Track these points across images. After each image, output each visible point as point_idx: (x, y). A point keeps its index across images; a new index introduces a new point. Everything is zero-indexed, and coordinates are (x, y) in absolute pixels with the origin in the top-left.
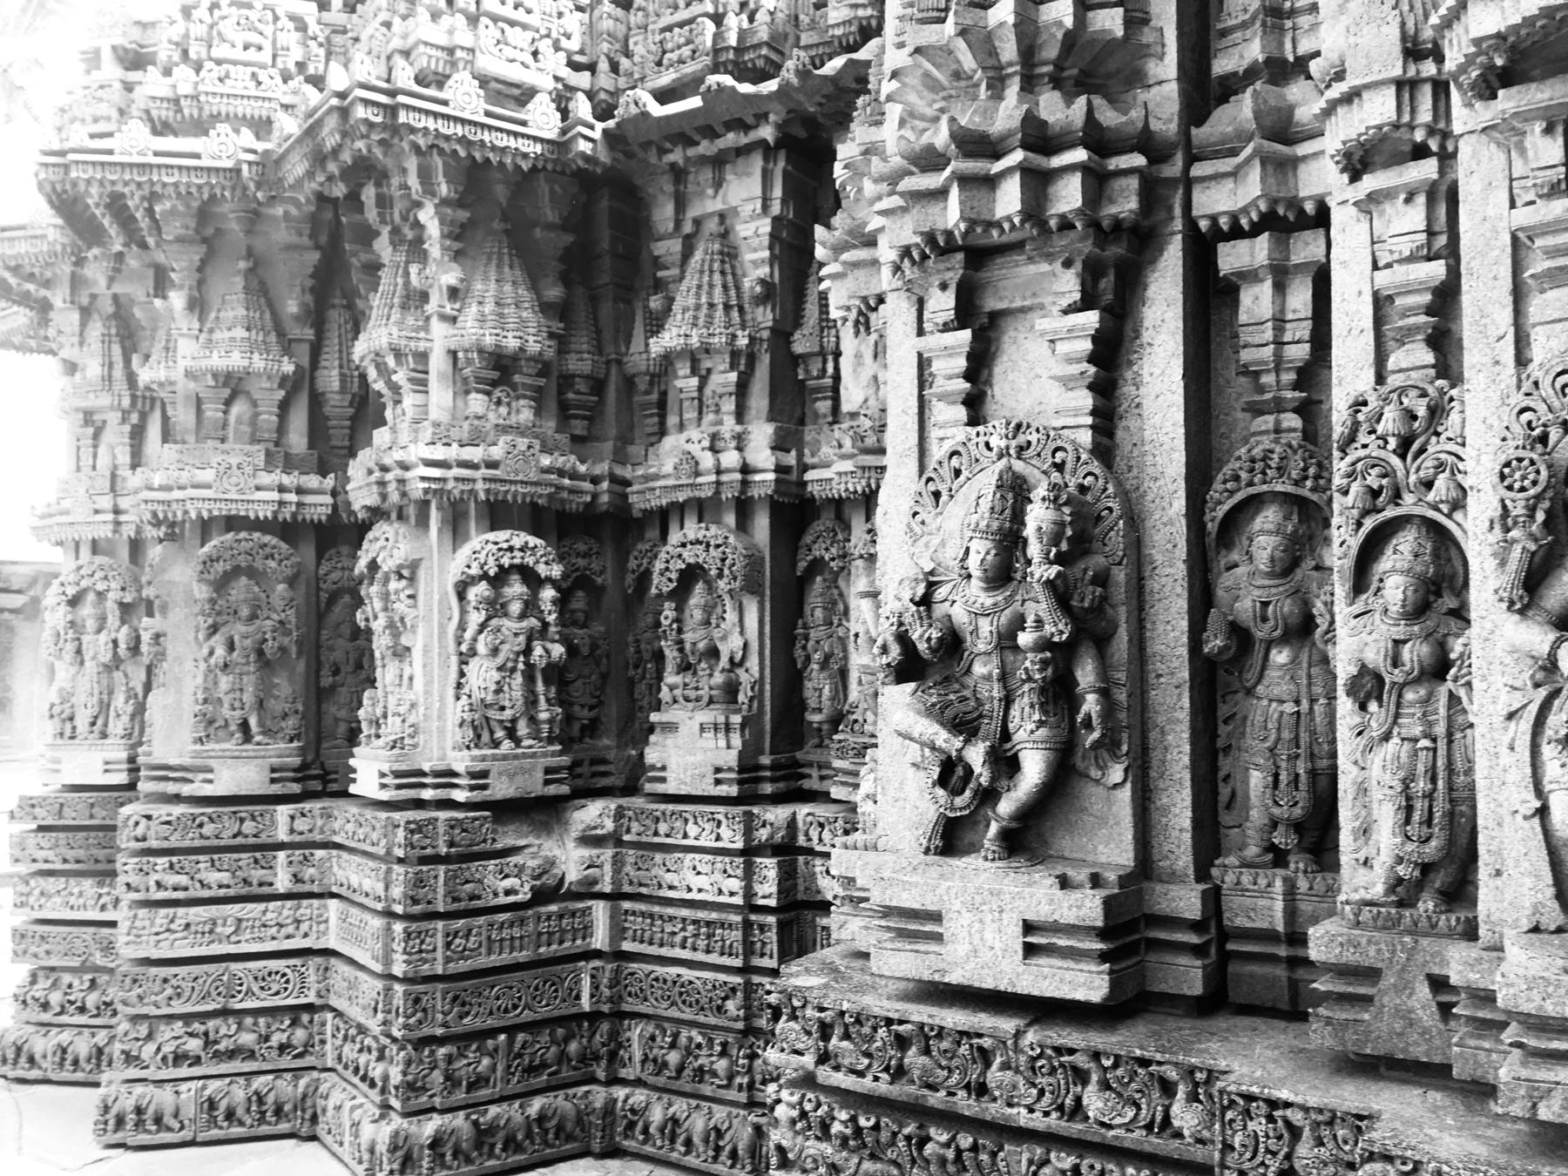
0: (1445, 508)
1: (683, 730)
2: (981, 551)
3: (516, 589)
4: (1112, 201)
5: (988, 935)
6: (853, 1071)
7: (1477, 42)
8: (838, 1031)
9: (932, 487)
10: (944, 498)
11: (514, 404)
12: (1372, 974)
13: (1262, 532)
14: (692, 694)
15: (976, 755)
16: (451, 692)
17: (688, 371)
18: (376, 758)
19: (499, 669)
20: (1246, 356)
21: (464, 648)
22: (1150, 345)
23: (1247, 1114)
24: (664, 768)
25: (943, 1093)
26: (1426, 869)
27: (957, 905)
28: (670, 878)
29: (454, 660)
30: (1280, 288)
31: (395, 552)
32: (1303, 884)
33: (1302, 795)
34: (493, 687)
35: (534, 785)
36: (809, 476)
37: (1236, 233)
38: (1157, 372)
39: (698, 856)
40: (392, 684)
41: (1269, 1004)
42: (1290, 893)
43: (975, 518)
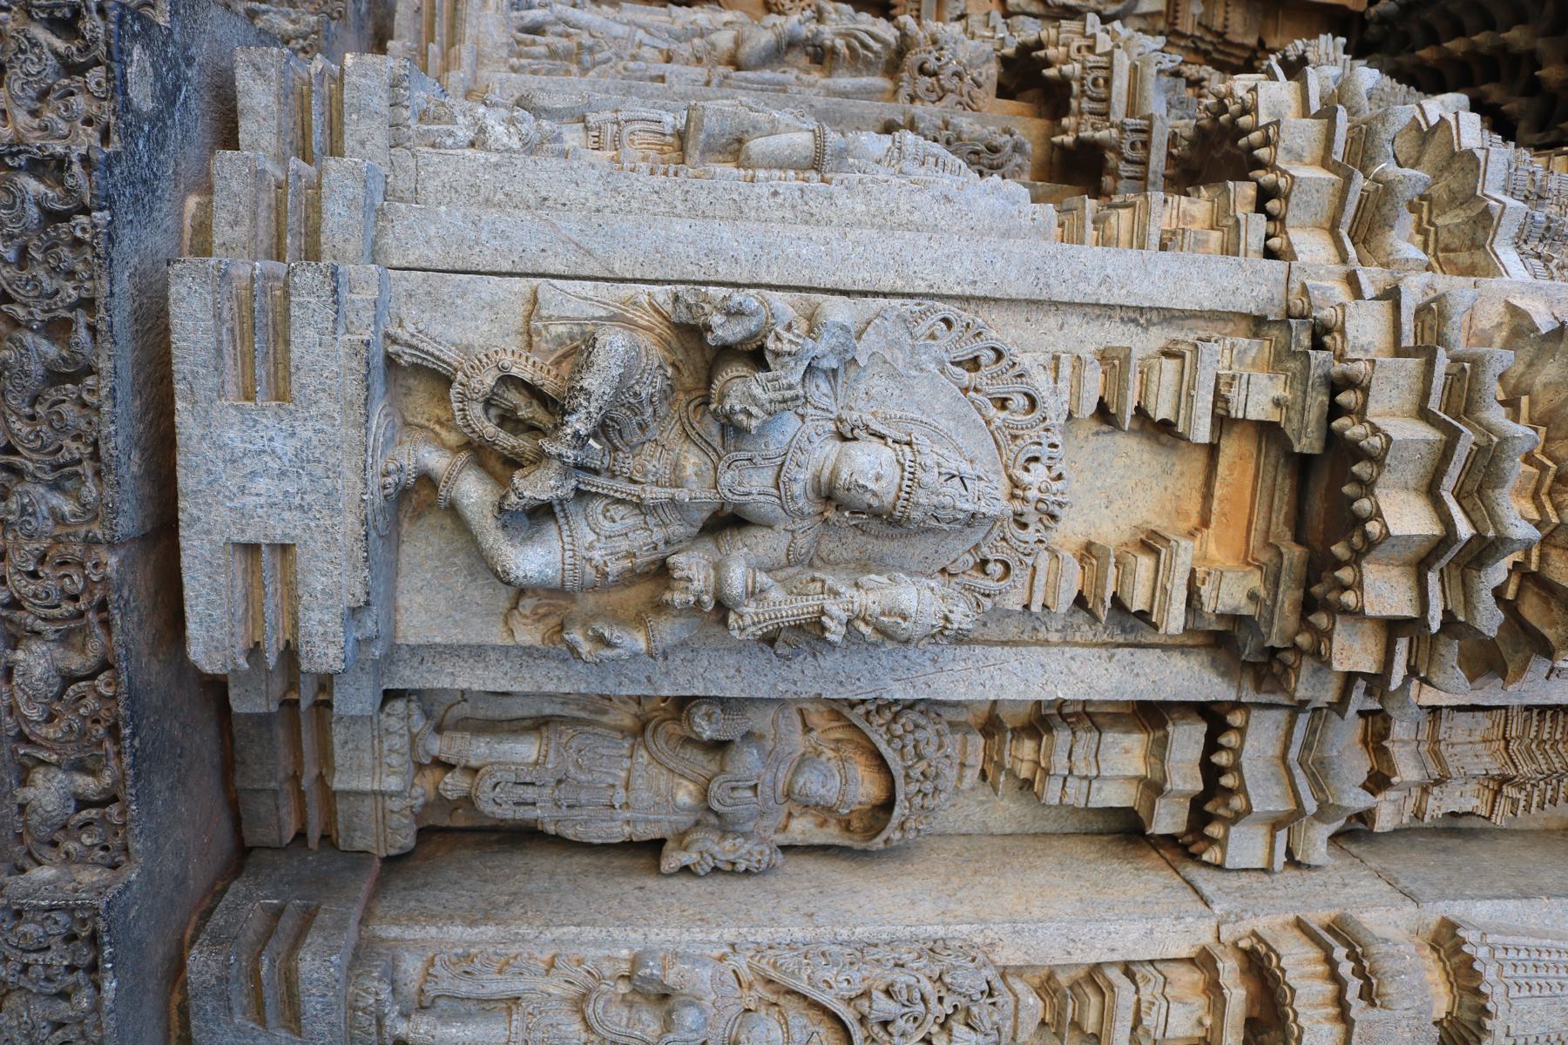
5: (262, 484)
9: (987, 357)
10: (967, 377)
22: (1111, 657)
32: (395, 804)
37: (1211, 746)
38: (1074, 666)
41: (238, 758)
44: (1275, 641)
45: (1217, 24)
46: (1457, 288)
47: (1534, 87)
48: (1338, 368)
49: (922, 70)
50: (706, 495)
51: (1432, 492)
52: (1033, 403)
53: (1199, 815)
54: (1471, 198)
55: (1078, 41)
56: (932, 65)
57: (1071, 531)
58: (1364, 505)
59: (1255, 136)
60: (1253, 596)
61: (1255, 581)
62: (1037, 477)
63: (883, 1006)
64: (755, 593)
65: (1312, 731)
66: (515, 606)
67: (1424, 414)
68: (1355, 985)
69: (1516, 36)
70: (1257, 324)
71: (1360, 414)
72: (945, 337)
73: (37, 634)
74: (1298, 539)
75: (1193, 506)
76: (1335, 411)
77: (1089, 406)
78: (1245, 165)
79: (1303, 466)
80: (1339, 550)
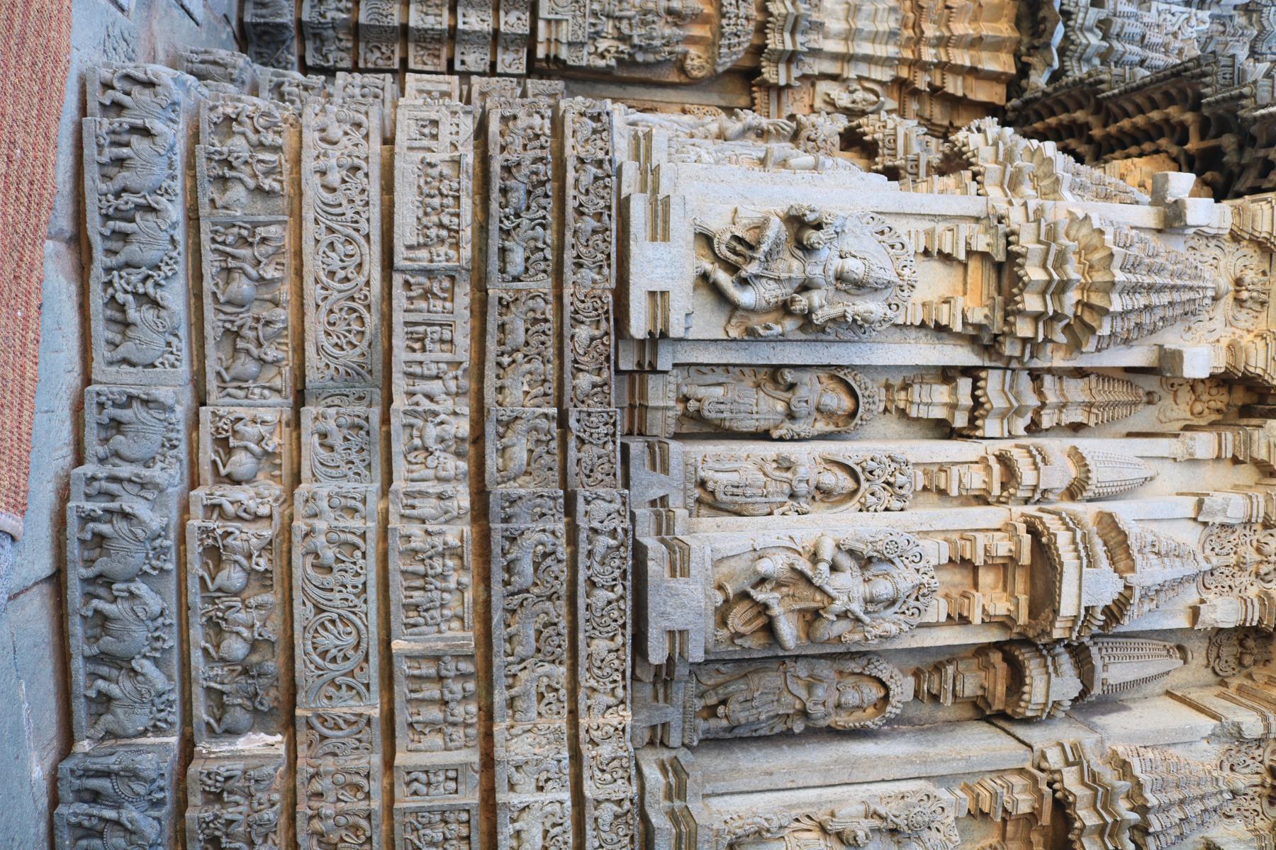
0: (863, 500)
2: (854, 267)
4: (1012, 343)
5: (659, 270)
6: (577, 180)
7: (1055, 535)
8: (600, 172)
9: (887, 230)
10: (880, 238)
12: (665, 470)
13: (840, 400)
15: (752, 269)
20: (916, 387)
23: (606, 424)
25: (573, 241)
26: (713, 493)
27: (674, 251)
30: (945, 404)
32: (670, 413)
33: (713, 415)
37: (975, 388)
42: (667, 408)
43: (874, 268)
44: (996, 331)
45: (927, 115)
46: (1048, 204)
47: (1090, 140)
48: (1008, 230)
49: (809, 139)
50: (802, 276)
51: (1044, 267)
52: (903, 246)
53: (972, 420)
54: (1052, 174)
55: (878, 124)
56: (813, 137)
57: (918, 296)
58: (1021, 272)
59: (969, 154)
60: (986, 316)
61: (986, 311)
62: (906, 272)
63: (873, 465)
64: (821, 307)
65: (1012, 380)
66: (729, 322)
67: (1039, 242)
68: (1039, 459)
69: (1079, 115)
70: (977, 219)
71: (1017, 243)
72: (873, 223)
73: (582, 323)
74: (999, 294)
75: (960, 287)
76: (1009, 243)
77: (922, 250)
78: (967, 164)
79: (999, 267)
80: (1015, 290)
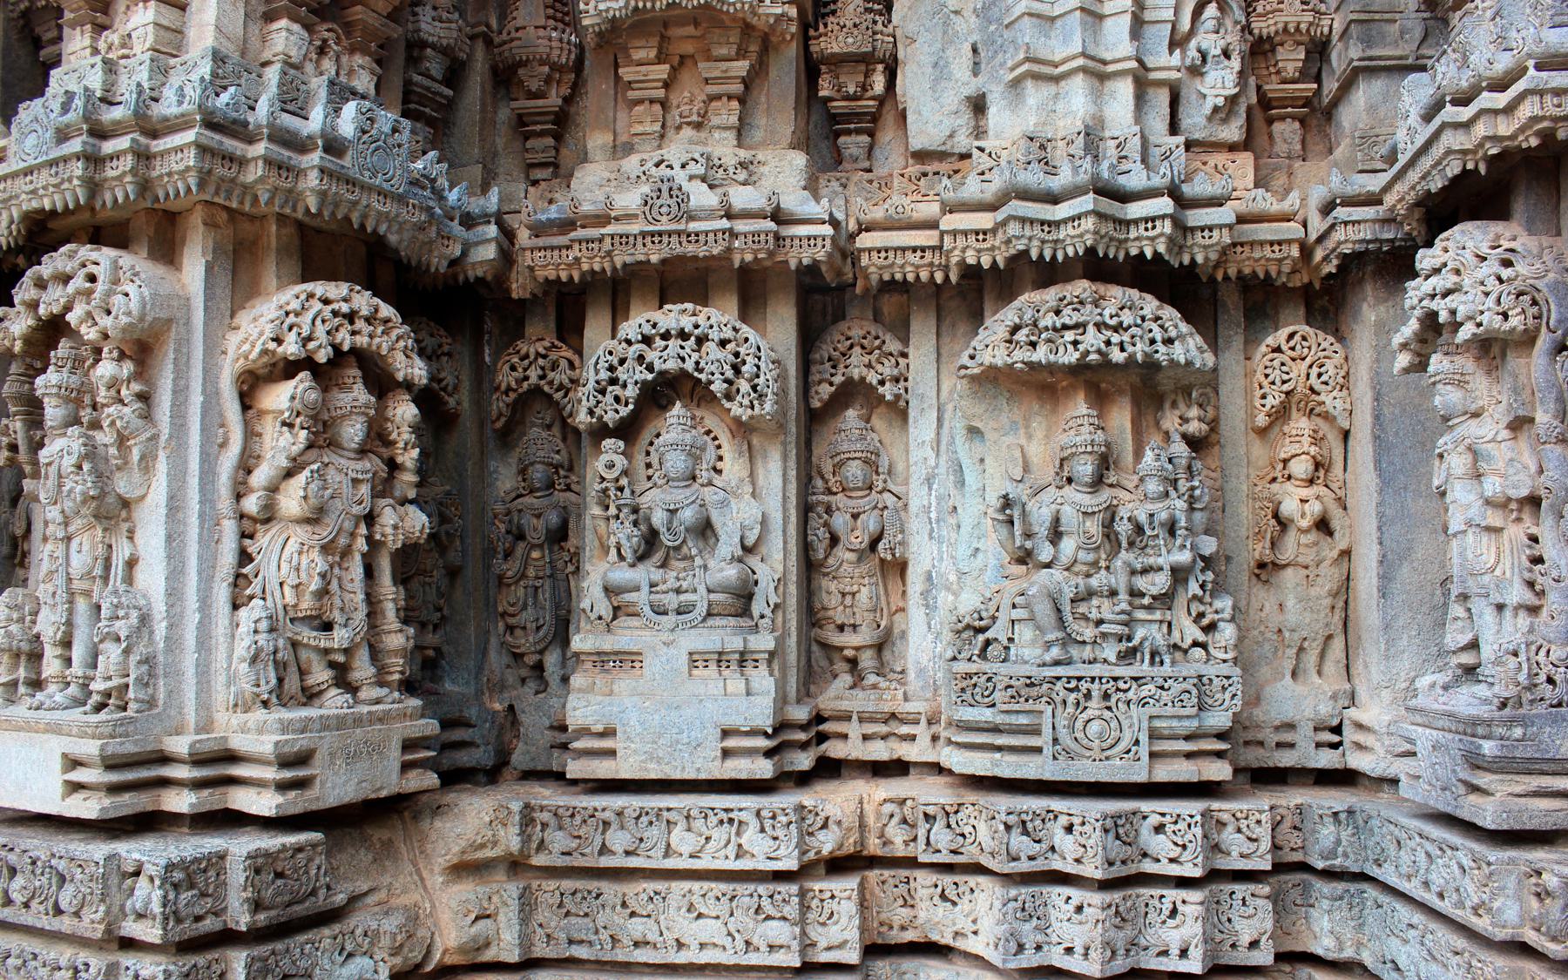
1: (653, 666)
3: (356, 395)
11: (345, 59)
14: (672, 601)
16: (222, 593)
17: (653, 54)
18: (55, 729)
19: (326, 549)
21: (251, 504)
24: (609, 733)
28: (637, 928)
29: (229, 528)
31: (118, 300)
34: (315, 584)
35: (387, 778)
36: (865, 240)
39: (696, 886)
40: (88, 575)
